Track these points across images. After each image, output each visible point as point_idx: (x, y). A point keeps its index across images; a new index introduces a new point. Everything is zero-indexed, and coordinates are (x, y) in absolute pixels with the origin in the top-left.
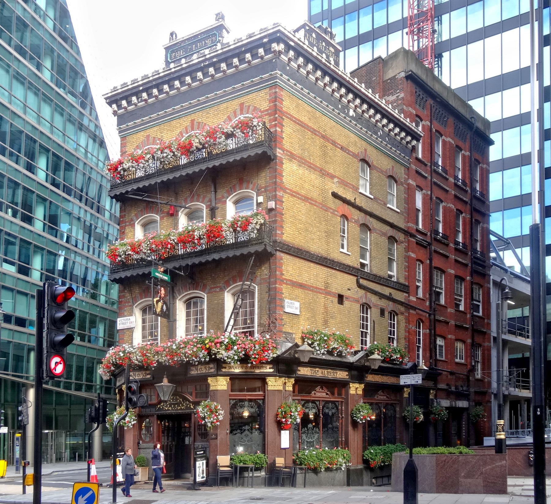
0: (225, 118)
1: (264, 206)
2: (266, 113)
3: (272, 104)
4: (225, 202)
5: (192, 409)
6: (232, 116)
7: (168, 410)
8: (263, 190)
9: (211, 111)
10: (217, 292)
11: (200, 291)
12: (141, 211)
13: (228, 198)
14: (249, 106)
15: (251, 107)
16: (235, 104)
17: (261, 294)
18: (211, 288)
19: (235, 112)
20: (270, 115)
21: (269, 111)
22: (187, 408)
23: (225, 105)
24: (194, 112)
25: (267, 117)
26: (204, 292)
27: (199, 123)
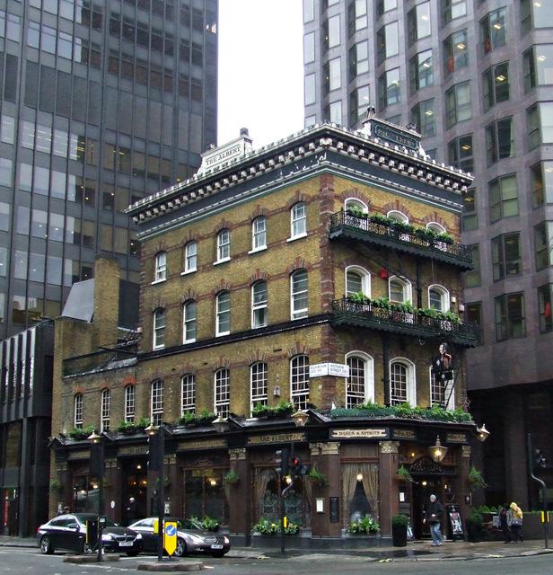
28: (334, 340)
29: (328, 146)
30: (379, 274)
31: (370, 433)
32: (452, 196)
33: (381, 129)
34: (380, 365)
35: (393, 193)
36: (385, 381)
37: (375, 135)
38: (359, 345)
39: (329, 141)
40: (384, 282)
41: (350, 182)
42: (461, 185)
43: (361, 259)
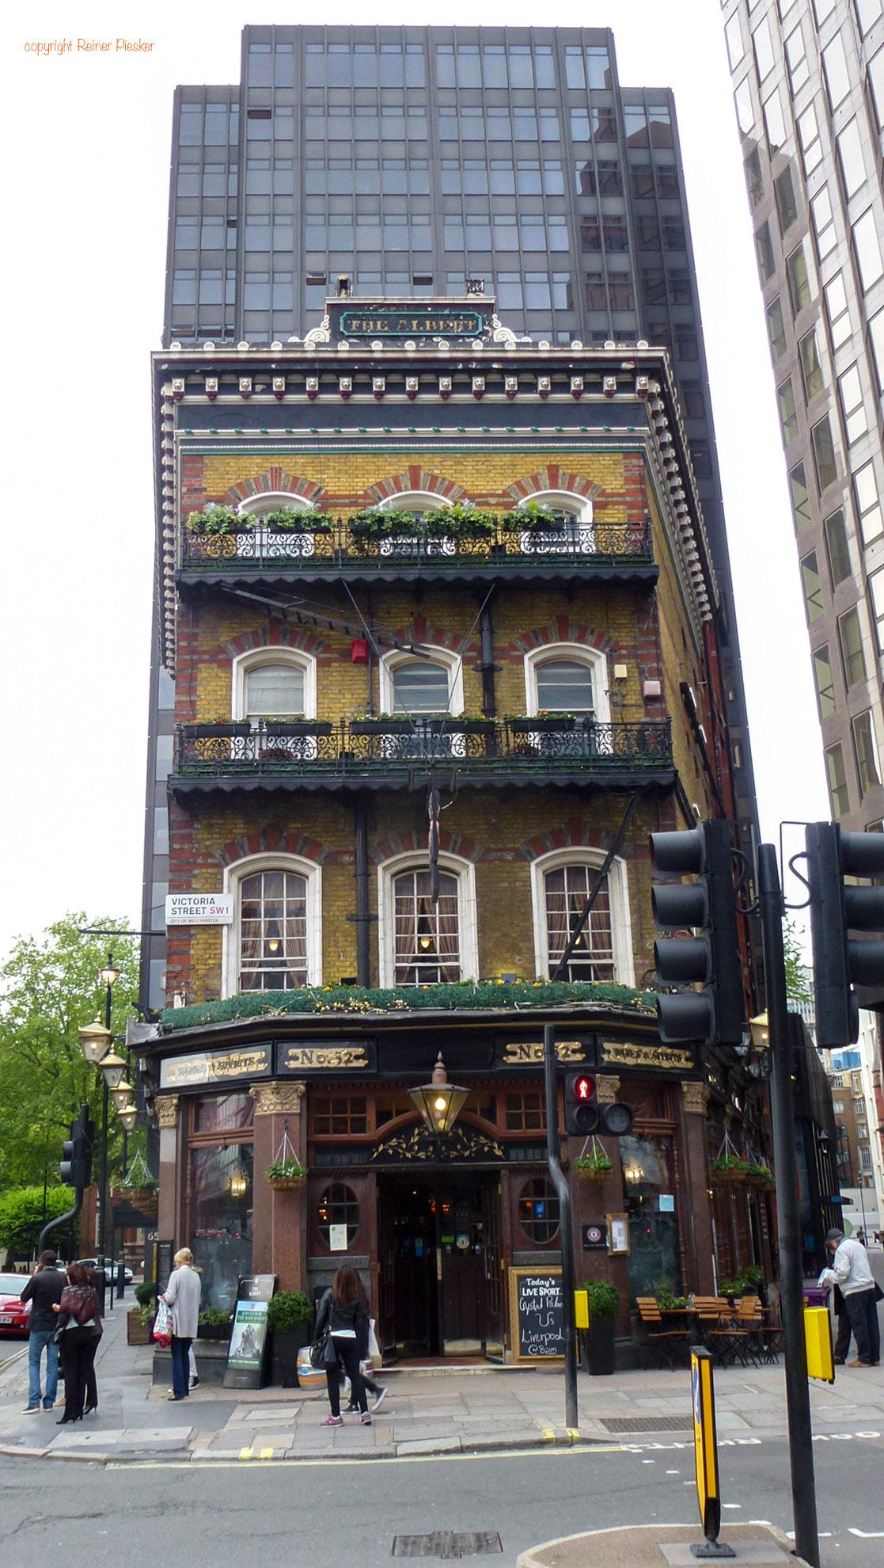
1: (633, 686)
2: (620, 499)
3: (633, 486)
4: (521, 660)
5: (499, 1158)
6: (528, 483)
7: (415, 1159)
8: (624, 652)
9: (470, 462)
10: (508, 861)
11: (453, 852)
12: (255, 633)
13: (527, 651)
14: (572, 478)
15: (578, 479)
16: (538, 464)
17: (638, 881)
18: (489, 851)
20: (631, 506)
21: (628, 499)
22: (480, 1155)
23: (507, 458)
24: (420, 452)
25: (621, 507)
26: (466, 857)
27: (434, 478)
28: (189, 838)
29: (179, 396)
30: (345, 656)
32: (609, 413)
33: (356, 317)
36: (367, 920)
37: (337, 335)
38: (272, 837)
39: (178, 382)
43: (280, 630)
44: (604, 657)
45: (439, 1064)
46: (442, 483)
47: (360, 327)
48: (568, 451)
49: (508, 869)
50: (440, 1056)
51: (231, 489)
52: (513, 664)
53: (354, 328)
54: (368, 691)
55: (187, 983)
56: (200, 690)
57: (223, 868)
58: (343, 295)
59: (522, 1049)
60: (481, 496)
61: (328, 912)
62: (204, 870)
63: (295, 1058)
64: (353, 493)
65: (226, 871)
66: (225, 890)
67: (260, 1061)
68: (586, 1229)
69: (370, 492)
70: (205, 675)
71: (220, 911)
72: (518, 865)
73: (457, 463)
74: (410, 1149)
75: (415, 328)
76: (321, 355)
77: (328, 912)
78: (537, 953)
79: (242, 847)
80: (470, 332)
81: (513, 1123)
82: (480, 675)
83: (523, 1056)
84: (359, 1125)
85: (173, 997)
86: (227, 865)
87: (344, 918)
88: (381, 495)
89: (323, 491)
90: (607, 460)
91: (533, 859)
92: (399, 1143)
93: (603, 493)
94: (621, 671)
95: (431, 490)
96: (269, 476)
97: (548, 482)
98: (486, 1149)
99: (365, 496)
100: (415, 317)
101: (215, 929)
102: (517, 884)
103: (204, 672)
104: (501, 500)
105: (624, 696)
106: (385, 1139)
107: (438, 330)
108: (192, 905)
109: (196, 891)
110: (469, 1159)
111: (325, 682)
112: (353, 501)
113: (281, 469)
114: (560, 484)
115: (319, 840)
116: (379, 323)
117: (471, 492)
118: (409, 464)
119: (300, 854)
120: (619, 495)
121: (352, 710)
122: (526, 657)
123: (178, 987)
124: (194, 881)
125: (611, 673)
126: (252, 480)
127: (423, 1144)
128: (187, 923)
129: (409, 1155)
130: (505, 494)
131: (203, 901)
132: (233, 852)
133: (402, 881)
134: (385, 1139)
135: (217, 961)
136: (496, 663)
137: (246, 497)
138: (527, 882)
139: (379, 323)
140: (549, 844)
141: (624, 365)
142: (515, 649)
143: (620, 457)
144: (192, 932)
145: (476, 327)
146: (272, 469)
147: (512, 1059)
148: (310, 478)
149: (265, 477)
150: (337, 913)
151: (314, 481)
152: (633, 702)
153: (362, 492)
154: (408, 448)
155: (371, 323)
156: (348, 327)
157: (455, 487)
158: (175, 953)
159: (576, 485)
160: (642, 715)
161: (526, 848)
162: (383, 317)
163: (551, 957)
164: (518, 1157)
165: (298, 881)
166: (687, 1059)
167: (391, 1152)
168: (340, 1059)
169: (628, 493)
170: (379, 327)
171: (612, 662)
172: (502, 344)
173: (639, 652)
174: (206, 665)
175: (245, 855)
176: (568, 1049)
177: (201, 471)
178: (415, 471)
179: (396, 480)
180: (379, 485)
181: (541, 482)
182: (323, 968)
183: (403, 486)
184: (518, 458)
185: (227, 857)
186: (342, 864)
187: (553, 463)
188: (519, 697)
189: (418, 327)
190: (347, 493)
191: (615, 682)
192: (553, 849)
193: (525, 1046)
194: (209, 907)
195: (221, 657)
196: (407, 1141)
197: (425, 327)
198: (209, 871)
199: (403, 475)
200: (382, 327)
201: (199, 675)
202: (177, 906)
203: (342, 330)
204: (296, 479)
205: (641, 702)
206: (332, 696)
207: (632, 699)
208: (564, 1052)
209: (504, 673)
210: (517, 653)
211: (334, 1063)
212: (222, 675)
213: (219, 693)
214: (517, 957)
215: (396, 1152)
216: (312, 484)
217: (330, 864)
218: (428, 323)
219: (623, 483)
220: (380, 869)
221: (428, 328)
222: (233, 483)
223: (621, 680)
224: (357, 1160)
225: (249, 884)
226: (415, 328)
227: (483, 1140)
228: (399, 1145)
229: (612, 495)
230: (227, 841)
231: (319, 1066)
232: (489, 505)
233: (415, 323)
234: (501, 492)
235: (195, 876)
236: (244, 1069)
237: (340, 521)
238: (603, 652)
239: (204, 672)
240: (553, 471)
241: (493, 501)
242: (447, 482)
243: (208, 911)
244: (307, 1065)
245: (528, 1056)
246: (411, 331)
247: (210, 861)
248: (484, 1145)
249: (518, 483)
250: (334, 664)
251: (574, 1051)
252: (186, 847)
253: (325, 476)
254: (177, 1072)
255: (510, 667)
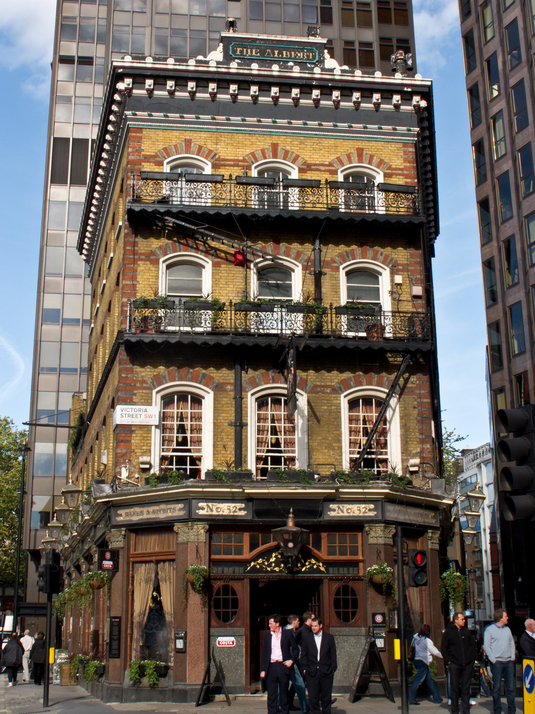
0: (333, 158)
2: (400, 172)
3: (408, 165)
4: (337, 269)
5: (322, 572)
6: (344, 159)
7: (273, 571)
8: (400, 267)
9: (309, 142)
10: (327, 393)
13: (341, 264)
14: (372, 157)
15: (375, 158)
16: (350, 147)
19: (349, 156)
21: (405, 172)
23: (332, 142)
24: (278, 135)
25: (401, 177)
27: (286, 152)
31: (165, 511)
34: (229, 399)
35: (264, 134)
37: (228, 58)
40: (240, 269)
41: (176, 133)
42: (407, 97)
44: (388, 270)
45: (291, 515)
46: (291, 155)
47: (242, 52)
48: (369, 140)
49: (327, 398)
50: (291, 510)
51: (159, 151)
52: (333, 271)
53: (238, 53)
54: (244, 284)
55: (130, 460)
56: (139, 278)
57: (151, 389)
58: (231, 31)
59: (339, 508)
60: (315, 165)
61: (217, 420)
62: (140, 391)
63: (203, 509)
64: (236, 158)
65: (154, 392)
66: (154, 403)
67: (180, 510)
68: (374, 615)
69: (247, 158)
70: (142, 268)
71: (150, 416)
72: (333, 395)
73: (301, 143)
74: (269, 565)
75: (276, 55)
76: (220, 70)
77: (217, 420)
78: (343, 450)
79: (164, 378)
80: (310, 60)
81: (331, 552)
82: (313, 277)
83: (340, 511)
84: (239, 551)
85: (121, 469)
86: (155, 388)
87: (227, 424)
88: (253, 160)
89: (217, 156)
90: (393, 147)
91: (342, 392)
92: (263, 562)
93: (390, 168)
94: (398, 279)
95: (284, 159)
96: (184, 144)
97: (356, 158)
98: (315, 567)
99: (244, 160)
100: (276, 49)
101: (147, 428)
102: (333, 408)
103: (142, 266)
104: (328, 168)
105: (400, 295)
106: (255, 559)
107: (290, 58)
108: (133, 412)
109: (135, 404)
110: (305, 572)
111: (217, 277)
112: (236, 163)
113: (191, 140)
114: (364, 160)
115: (212, 375)
116: (254, 51)
117: (309, 162)
118: (271, 142)
119: (200, 383)
120: (400, 169)
121: (234, 295)
122: (341, 267)
123: (124, 463)
124: (134, 397)
125: (392, 280)
126: (173, 147)
127: (277, 564)
128: (130, 423)
129: (269, 569)
130: (330, 165)
131: (140, 410)
132: (158, 380)
133: (262, 403)
134: (255, 559)
135: (149, 448)
136: (323, 270)
137: (169, 156)
138: (338, 406)
139: (254, 51)
140: (352, 383)
141: (405, 89)
142: (335, 262)
143: (401, 145)
144: (133, 429)
145: (314, 57)
146: (185, 139)
147: (332, 514)
148: (209, 146)
149: (181, 144)
150: (223, 421)
151: (212, 149)
152: (405, 299)
153: (242, 158)
154: (271, 132)
155: (249, 50)
156: (234, 52)
157: (300, 158)
158: (122, 441)
159: (374, 161)
160: (410, 307)
161: (338, 386)
162: (257, 47)
163: (351, 453)
164: (333, 572)
165: (197, 400)
166: (432, 517)
167: (258, 567)
168: (229, 509)
169: (405, 168)
170: (254, 54)
171: (393, 273)
172: (332, 70)
173: (410, 268)
174: (143, 262)
175: (166, 382)
176: (366, 509)
177: (141, 138)
178: (275, 147)
179: (263, 151)
180: (253, 154)
181: (352, 158)
182: (214, 454)
183: (267, 155)
184: (339, 142)
185: (155, 383)
186: (226, 390)
187: (361, 147)
188: (336, 292)
189: (278, 55)
190: (233, 158)
191: (395, 286)
192: (355, 387)
193: (341, 506)
194: (143, 414)
195: (153, 257)
196: (268, 560)
197: (283, 55)
198: (144, 391)
199: (267, 149)
200: (256, 53)
201: (138, 268)
202: (124, 412)
203: (231, 53)
204: (200, 147)
205: (410, 299)
206: (221, 286)
207: (405, 297)
208: (364, 510)
209: (327, 276)
210: (336, 265)
211: (226, 513)
212: (153, 269)
213: (151, 280)
214: (332, 452)
215: (261, 567)
216: (210, 151)
217: (218, 389)
218: (284, 53)
219: (402, 162)
220: (249, 394)
221: (284, 56)
222: (161, 147)
223: (399, 284)
224: (239, 571)
225: (167, 401)
226: (276, 55)
227: (313, 561)
228: (263, 563)
229: (396, 169)
230: (155, 374)
231: (217, 513)
232: (320, 170)
233: (276, 52)
234: (327, 163)
235: (135, 394)
236: (170, 514)
237: (231, 176)
238: (387, 266)
239: (142, 266)
240: (360, 152)
241: (322, 168)
242: (294, 155)
243: (143, 416)
244: (210, 513)
245: (342, 512)
246: (274, 57)
247: (144, 385)
248: (314, 564)
249: (338, 159)
250: (222, 266)
251: (370, 510)
252: (129, 376)
253: (218, 146)
254: (124, 515)
255: (331, 273)
